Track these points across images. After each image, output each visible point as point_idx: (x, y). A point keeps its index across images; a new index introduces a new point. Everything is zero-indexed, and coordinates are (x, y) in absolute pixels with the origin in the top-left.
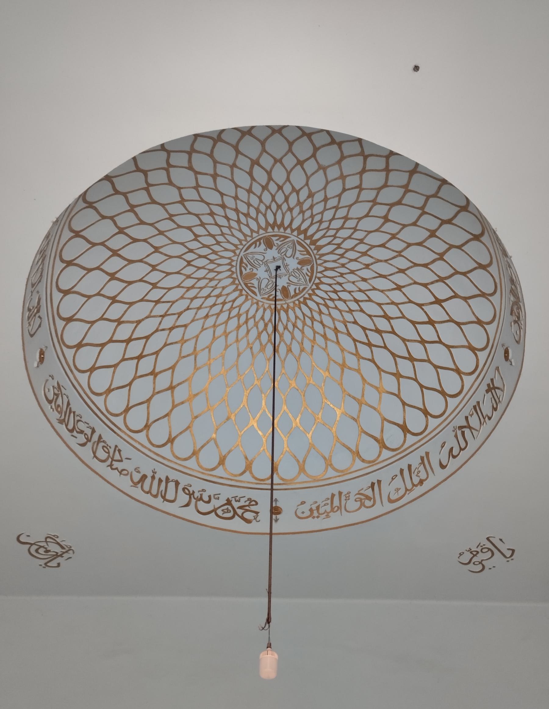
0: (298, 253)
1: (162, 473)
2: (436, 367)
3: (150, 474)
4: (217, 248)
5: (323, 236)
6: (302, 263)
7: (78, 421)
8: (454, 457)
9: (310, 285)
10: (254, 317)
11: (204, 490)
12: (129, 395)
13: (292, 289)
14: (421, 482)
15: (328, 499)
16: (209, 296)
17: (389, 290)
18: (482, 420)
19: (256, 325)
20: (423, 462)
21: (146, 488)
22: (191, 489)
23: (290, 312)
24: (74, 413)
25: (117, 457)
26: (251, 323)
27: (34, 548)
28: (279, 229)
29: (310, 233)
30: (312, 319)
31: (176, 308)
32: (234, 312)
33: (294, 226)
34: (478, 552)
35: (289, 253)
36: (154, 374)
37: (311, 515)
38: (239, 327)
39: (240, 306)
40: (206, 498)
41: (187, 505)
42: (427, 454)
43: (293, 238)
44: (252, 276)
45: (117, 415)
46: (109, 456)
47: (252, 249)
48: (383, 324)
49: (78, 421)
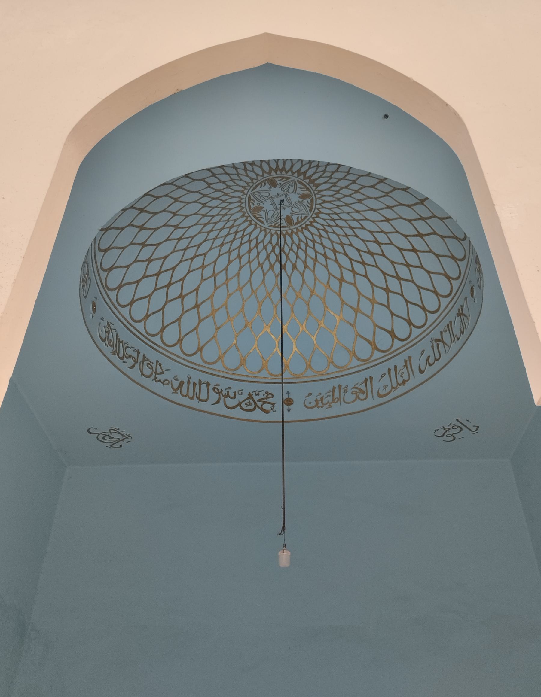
1: (195, 379)
2: (419, 287)
3: (186, 380)
4: (227, 191)
5: (321, 177)
6: (303, 197)
7: (127, 347)
8: (431, 365)
9: (311, 214)
10: (263, 241)
12: (163, 318)
13: (295, 218)
14: (404, 382)
15: (330, 391)
16: (223, 228)
17: (379, 221)
18: (453, 339)
19: (265, 247)
20: (406, 365)
21: (184, 393)
22: (219, 388)
23: (294, 236)
24: (122, 342)
25: (159, 370)
26: (261, 246)
27: (100, 437)
28: (281, 172)
29: (308, 174)
30: (314, 241)
31: (196, 241)
32: (246, 239)
34: (449, 429)
36: (182, 297)
37: (317, 405)
38: (250, 250)
39: (250, 234)
40: (232, 395)
41: (218, 402)
42: (410, 358)
43: (293, 178)
44: (260, 209)
45: (155, 335)
46: (153, 370)
47: (258, 189)
48: (374, 248)
49: (127, 347)
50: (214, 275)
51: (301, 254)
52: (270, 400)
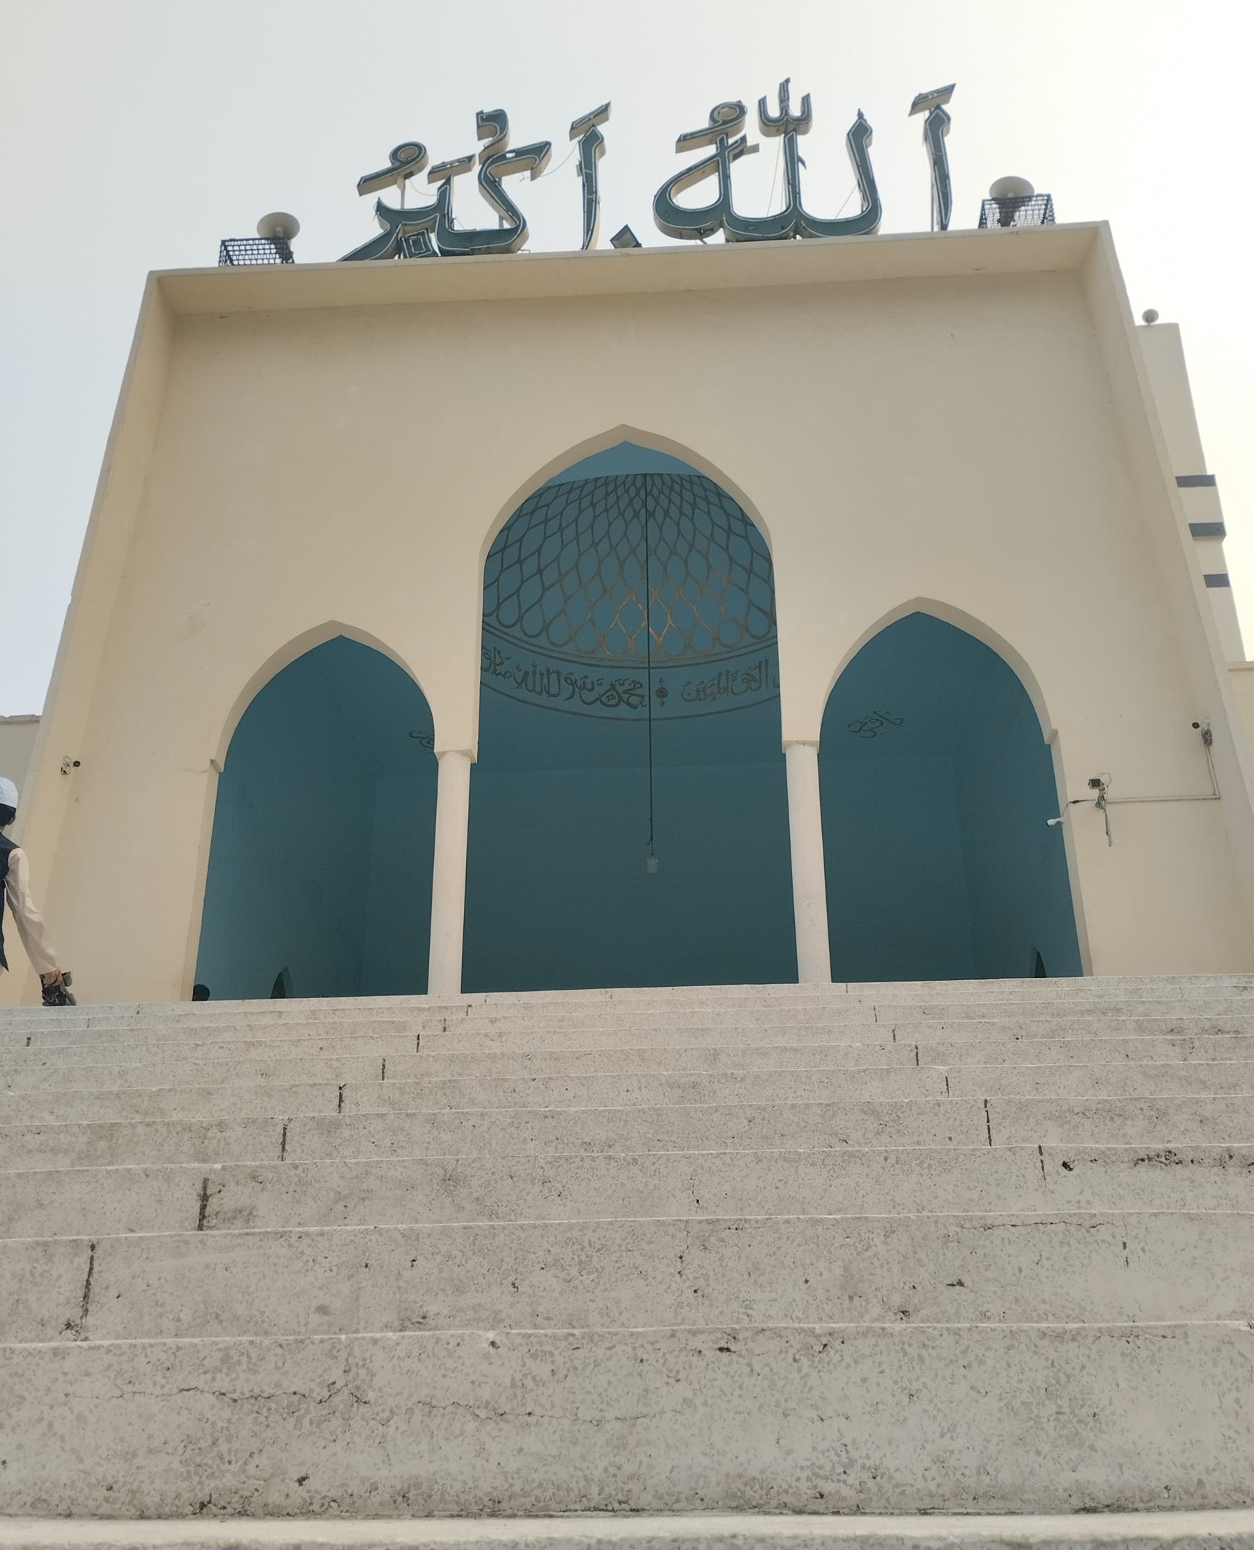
11: (586, 677)
19: (627, 491)
26: (621, 490)
36: (520, 562)
38: (607, 495)
40: (589, 686)
41: (572, 697)
50: (561, 530)
52: (638, 691)
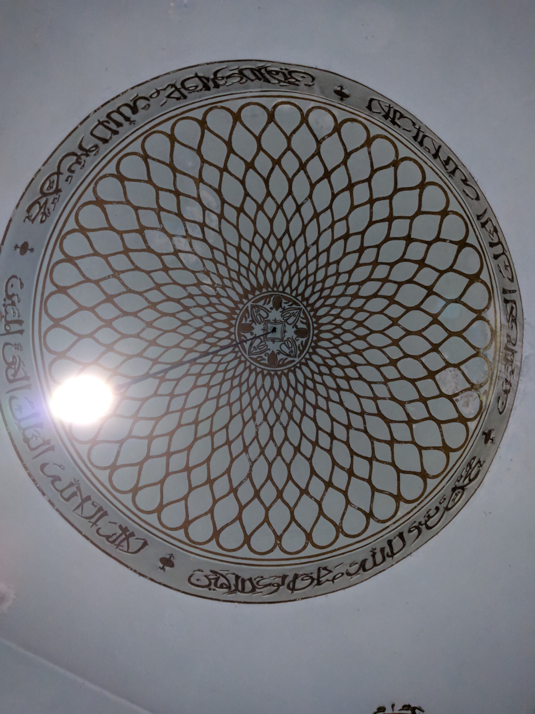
0: (265, 306)
9: (302, 306)
10: (313, 372)
13: (300, 325)
19: (321, 374)
23: (322, 335)
26: (318, 378)
30: (337, 316)
33: (237, 298)
35: (264, 314)
39: (297, 380)
43: (249, 304)
51: (347, 337)
